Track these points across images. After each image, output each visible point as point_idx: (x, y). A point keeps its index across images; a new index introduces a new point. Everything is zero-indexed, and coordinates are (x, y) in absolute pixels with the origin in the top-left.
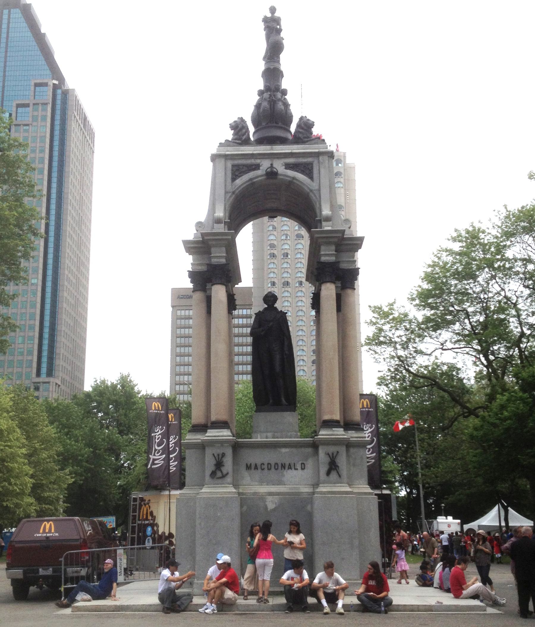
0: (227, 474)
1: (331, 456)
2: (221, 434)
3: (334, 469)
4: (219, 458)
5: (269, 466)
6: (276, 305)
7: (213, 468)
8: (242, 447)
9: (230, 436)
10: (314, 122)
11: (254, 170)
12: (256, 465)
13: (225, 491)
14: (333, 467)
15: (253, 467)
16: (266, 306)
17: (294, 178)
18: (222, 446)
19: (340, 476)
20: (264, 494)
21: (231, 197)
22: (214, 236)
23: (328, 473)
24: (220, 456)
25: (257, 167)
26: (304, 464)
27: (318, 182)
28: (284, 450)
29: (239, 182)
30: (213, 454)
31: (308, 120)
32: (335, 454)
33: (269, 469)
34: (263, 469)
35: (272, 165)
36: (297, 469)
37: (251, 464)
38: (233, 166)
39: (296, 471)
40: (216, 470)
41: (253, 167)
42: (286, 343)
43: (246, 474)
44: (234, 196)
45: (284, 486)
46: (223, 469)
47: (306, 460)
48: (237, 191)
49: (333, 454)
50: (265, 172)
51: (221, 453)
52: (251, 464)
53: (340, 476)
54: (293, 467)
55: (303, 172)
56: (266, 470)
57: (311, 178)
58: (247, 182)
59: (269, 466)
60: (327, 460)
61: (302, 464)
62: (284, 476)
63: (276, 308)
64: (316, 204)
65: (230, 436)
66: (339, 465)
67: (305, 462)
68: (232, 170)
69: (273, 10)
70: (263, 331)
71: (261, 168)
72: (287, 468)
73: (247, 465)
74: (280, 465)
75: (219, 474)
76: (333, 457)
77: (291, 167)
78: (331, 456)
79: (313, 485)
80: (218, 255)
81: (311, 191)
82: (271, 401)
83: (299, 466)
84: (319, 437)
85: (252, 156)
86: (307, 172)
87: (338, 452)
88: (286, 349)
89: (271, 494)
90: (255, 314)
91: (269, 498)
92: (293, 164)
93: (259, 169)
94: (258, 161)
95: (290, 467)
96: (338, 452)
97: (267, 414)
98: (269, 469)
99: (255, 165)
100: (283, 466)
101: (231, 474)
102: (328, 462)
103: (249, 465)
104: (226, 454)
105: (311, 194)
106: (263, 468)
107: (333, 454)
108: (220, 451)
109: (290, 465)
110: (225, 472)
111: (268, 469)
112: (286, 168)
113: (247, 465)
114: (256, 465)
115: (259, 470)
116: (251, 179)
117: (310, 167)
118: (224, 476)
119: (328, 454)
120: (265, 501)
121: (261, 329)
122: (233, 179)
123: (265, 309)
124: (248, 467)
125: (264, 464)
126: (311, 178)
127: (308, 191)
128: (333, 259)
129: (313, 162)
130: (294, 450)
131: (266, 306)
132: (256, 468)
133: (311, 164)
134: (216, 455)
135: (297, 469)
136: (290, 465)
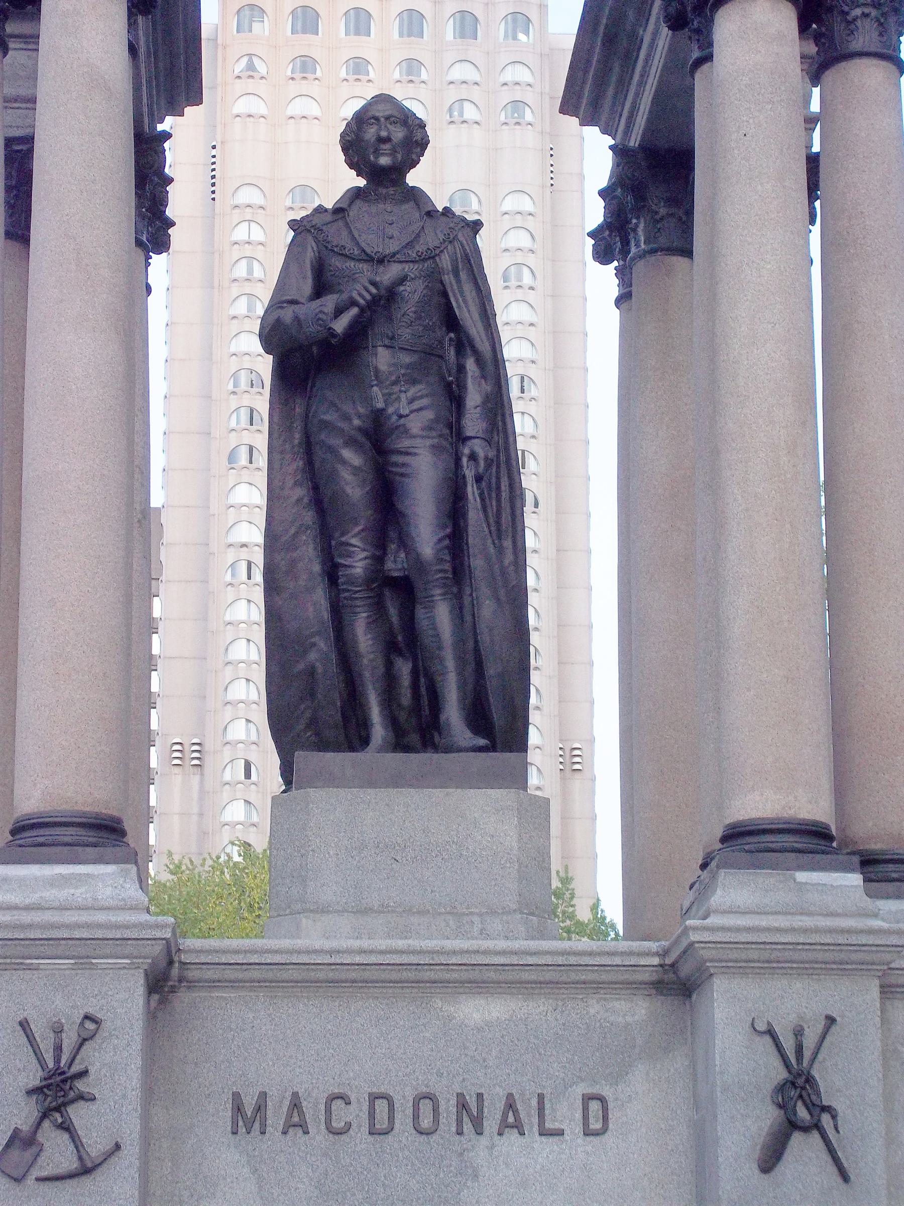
0: (118, 1147)
1: (789, 1046)
2: (80, 894)
3: (805, 1129)
4: (58, 1049)
5: (381, 1106)
6: (413, 178)
8: (214, 984)
9: (134, 908)
12: (296, 1105)
14: (802, 1113)
15: (276, 1117)
16: (361, 182)
18: (84, 962)
19: (844, 1176)
24: (69, 1041)
26: (601, 1099)
30: (24, 1025)
32: (809, 1043)
36: (560, 1133)
37: (263, 1095)
39: (545, 1147)
40: (39, 1124)
42: (474, 398)
46: (77, 1114)
49: (798, 1033)
52: (263, 1095)
53: (844, 1176)
54: (531, 1121)
56: (360, 1138)
59: (381, 1106)
63: (415, 196)
65: (134, 908)
67: (607, 1091)
72: (491, 1124)
73: (236, 1096)
74: (448, 1106)
78: (789, 1046)
84: (712, 920)
87: (831, 1020)
88: (473, 423)
90: (294, 225)
96: (831, 1020)
97: (370, 794)
101: (131, 1154)
102: (768, 1087)
106: (337, 1124)
107: (798, 1033)
109: (510, 1105)
110: (95, 1145)
113: (236, 1096)
114: (296, 1105)
115: (318, 1134)
118: (85, 1170)
119: (771, 1032)
121: (329, 302)
123: (356, 194)
131: (361, 182)
135: (560, 1133)
136: (510, 1105)
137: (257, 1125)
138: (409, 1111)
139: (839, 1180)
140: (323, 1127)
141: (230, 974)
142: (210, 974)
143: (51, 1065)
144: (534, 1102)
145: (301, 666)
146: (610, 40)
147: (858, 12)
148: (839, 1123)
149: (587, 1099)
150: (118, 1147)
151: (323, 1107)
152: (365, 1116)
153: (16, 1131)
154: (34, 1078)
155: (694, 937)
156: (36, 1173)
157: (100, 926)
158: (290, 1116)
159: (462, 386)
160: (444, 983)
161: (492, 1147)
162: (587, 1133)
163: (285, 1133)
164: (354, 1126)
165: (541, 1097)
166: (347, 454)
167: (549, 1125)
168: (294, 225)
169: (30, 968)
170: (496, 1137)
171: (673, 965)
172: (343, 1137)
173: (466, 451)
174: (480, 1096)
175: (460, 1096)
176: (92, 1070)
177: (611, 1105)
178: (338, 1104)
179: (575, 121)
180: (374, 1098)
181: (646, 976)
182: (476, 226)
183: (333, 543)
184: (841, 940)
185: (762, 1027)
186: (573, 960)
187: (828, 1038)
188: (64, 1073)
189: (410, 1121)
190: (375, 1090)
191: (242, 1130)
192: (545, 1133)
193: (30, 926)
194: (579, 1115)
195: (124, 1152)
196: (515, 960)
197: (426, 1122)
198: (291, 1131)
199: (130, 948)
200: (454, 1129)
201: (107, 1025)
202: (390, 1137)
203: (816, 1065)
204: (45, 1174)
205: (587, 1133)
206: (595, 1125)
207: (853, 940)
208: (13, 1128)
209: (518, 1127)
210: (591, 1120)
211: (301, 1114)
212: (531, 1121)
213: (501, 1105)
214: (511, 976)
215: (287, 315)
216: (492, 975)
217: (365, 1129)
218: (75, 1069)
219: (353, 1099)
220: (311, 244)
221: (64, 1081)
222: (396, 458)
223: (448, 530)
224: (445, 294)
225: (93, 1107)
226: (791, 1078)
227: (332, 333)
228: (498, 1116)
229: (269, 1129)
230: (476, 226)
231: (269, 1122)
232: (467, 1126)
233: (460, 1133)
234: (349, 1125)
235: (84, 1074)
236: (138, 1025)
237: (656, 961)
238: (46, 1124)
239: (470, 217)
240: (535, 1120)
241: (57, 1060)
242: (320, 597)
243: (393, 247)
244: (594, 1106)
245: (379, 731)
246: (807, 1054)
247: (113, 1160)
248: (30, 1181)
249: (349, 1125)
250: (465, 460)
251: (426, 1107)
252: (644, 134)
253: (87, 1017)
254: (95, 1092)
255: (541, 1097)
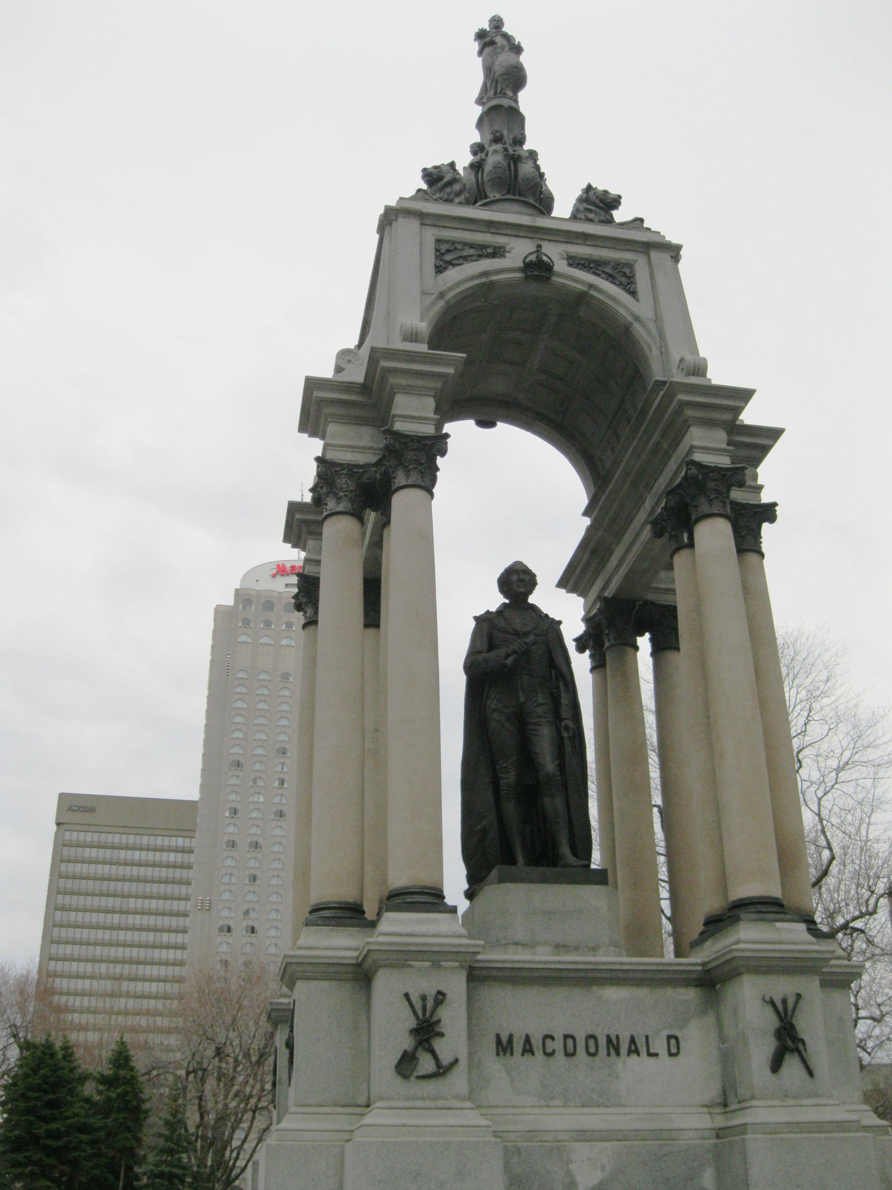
0: (457, 1061)
1: (780, 1007)
2: (431, 928)
5: (570, 1042)
7: (407, 1043)
9: (460, 936)
10: (620, 197)
11: (494, 255)
12: (528, 1040)
13: (452, 1122)
14: (790, 1043)
15: (518, 1047)
16: (507, 601)
17: (591, 286)
18: (436, 965)
19: (810, 1073)
20: (561, 1136)
21: (433, 303)
22: (406, 361)
23: (776, 1065)
24: (430, 1004)
25: (498, 252)
26: (676, 1038)
27: (651, 301)
28: (613, 993)
29: (453, 275)
30: (407, 996)
31: (606, 192)
33: (570, 1055)
34: (549, 1055)
35: (539, 246)
36: (656, 1055)
37: (511, 1037)
38: (438, 241)
40: (415, 1049)
41: (490, 250)
42: (565, 700)
43: (494, 1066)
44: (441, 303)
45: (619, 1110)
47: (682, 1027)
48: (450, 295)
49: (784, 1001)
50: (520, 264)
51: (434, 992)
52: (511, 1037)
53: (810, 1073)
54: (643, 1049)
55: (610, 278)
57: (633, 293)
58: (472, 278)
59: (570, 1042)
60: (771, 1021)
61: (669, 1037)
62: (618, 1077)
63: (533, 608)
64: (650, 350)
65: (460, 936)
66: (806, 1039)
67: (678, 1034)
68: (437, 250)
69: (497, 23)
70: (507, 656)
71: (508, 255)
72: (624, 1050)
73: (498, 1037)
74: (602, 1042)
75: (426, 1064)
76: (785, 1010)
77: (583, 265)
78: (780, 1007)
79: (708, 1106)
80: (416, 414)
81: (637, 319)
82: (520, 859)
83: (659, 1045)
85: (491, 226)
86: (624, 280)
87: (799, 996)
89: (584, 1136)
90: (476, 618)
91: (582, 1151)
92: (586, 259)
93: (503, 256)
94: (500, 240)
95: (634, 1049)
96: (799, 996)
98: (570, 1055)
99: (494, 248)
100: (613, 1045)
103: (504, 1039)
104: (449, 997)
105: (637, 326)
106: (549, 1050)
107: (784, 1001)
108: (430, 988)
109: (633, 1040)
110: (446, 1059)
111: (567, 1054)
112: (570, 265)
113: (498, 1037)
114: (528, 1040)
115: (539, 1055)
116: (485, 274)
117: (628, 272)
118: (442, 1071)
119: (772, 1003)
120: (569, 1161)
121: (502, 652)
122: (439, 270)
123: (505, 605)
124: (504, 1047)
125: (552, 1038)
126: (633, 293)
127: (630, 319)
128: (724, 461)
129: (636, 261)
130: (643, 993)
131: (507, 601)
132: (528, 1049)
133: (630, 265)
134: (415, 999)
135: (656, 1055)
136: (633, 1040)
137: (509, 1050)
138: (583, 1044)
139: (808, 1076)
140: (541, 1052)
141: (494, 973)
142: (484, 973)
143: (421, 1016)
144: (644, 1040)
145: (479, 827)
146: (594, 552)
147: (745, 532)
148: (807, 1046)
149: (669, 1037)
150: (457, 1061)
151: (541, 1041)
152: (562, 1046)
153: (405, 1053)
154: (412, 1023)
155: (736, 954)
156: (415, 1074)
157: (446, 945)
158: (525, 1045)
159: (559, 696)
160: (598, 979)
161: (624, 1063)
162: (671, 1054)
163: (523, 1055)
164: (557, 1051)
165: (647, 1037)
166: (506, 724)
167: (652, 1051)
168: (476, 618)
169: (411, 967)
170: (626, 1057)
171: (709, 971)
172: (552, 1058)
173: (563, 724)
174: (617, 1037)
175: (609, 1038)
176: (442, 1020)
177: (680, 1040)
178: (548, 1041)
179: (564, 591)
180: (566, 1037)
181: (694, 976)
182: (560, 622)
183: (498, 767)
184: (804, 955)
185: (768, 999)
186: (661, 968)
187: (799, 1005)
188: (428, 1021)
189: (584, 1049)
190: (566, 1033)
191: (501, 1053)
192: (650, 1054)
193: (412, 944)
194: (665, 1045)
195: (460, 1062)
196: (634, 968)
197: (592, 1049)
198: (526, 1055)
199: (460, 957)
200: (605, 1053)
201: (449, 996)
202: (574, 1057)
203: (794, 1018)
204: (420, 1074)
205: (671, 1054)
206: (674, 1051)
207: (809, 956)
208: (403, 1050)
209: (637, 1052)
210: (672, 1048)
211: (531, 1045)
212: (643, 1049)
213: (628, 1040)
214: (631, 975)
215: (480, 657)
216: (621, 975)
217: (562, 1052)
218: (434, 1019)
219: (556, 1037)
220: (486, 625)
221: (429, 1026)
222: (530, 727)
223: (558, 762)
224: (550, 653)
225: (444, 1040)
226: (783, 1024)
227: (505, 666)
228: (627, 1046)
229: (515, 1053)
230: (560, 622)
231: (515, 1049)
232: (612, 1052)
233: (609, 1054)
234: (554, 1051)
235: (439, 1021)
236: (464, 997)
237: (700, 968)
238: (420, 1048)
239: (557, 619)
240: (645, 1048)
241: (424, 1014)
242: (489, 794)
243: (527, 629)
244: (673, 1041)
245: (520, 859)
246: (790, 1013)
247: (455, 1067)
248: (413, 1079)
249: (554, 1051)
250: (562, 729)
251: (591, 1042)
252: (616, 590)
253: (440, 993)
254: (444, 1031)
255: (647, 1037)
